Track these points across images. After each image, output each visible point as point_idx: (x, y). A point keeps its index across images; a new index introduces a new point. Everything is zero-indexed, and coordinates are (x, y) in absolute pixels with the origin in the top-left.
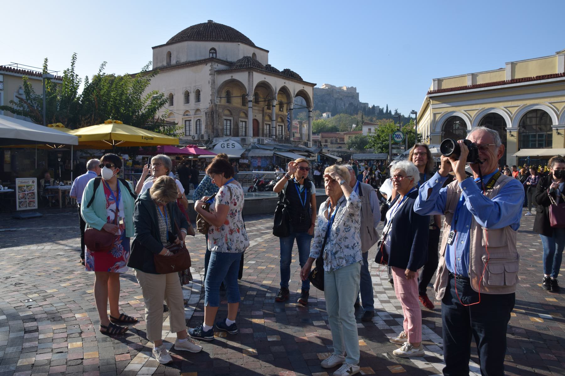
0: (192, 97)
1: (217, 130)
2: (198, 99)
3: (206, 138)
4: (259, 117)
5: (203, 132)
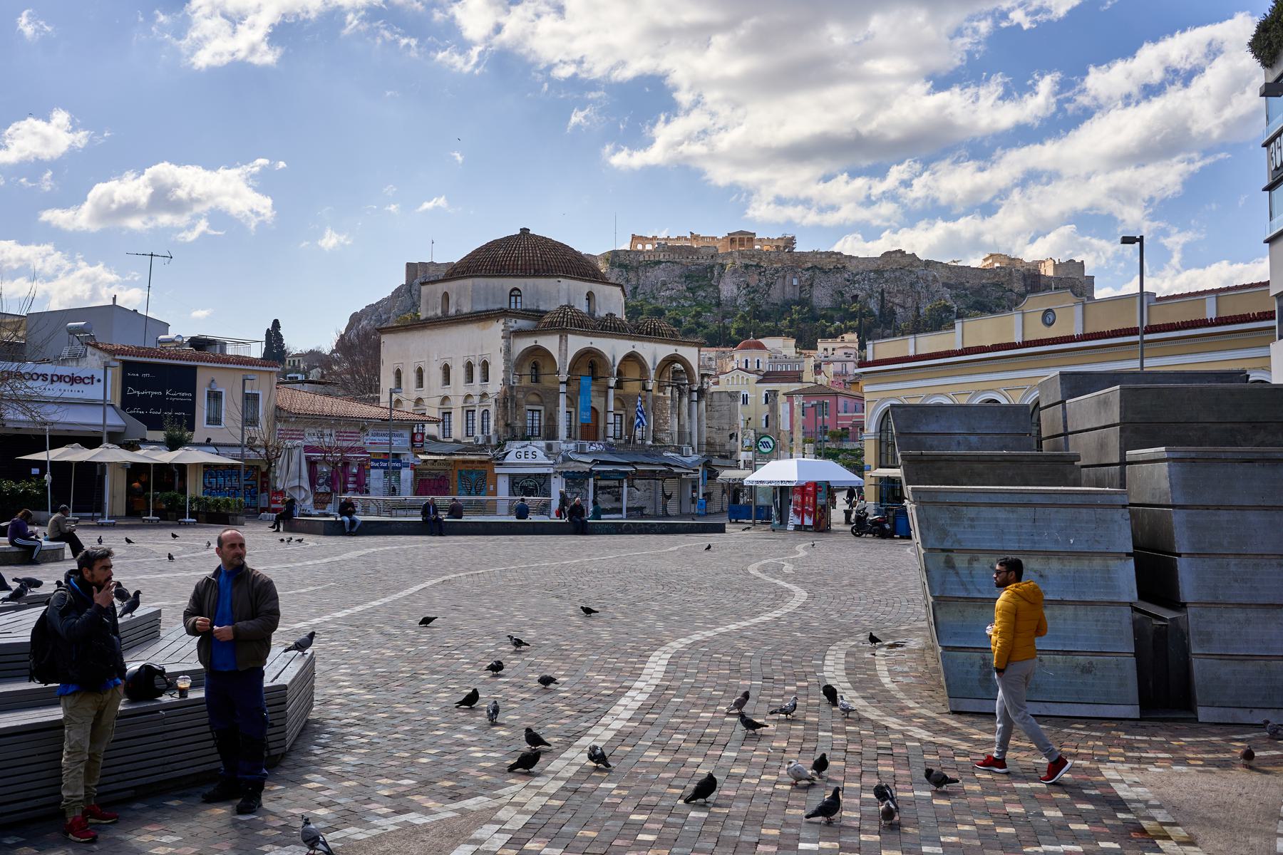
1: (513, 429)
3: (494, 442)
4: (598, 403)
5: (491, 433)
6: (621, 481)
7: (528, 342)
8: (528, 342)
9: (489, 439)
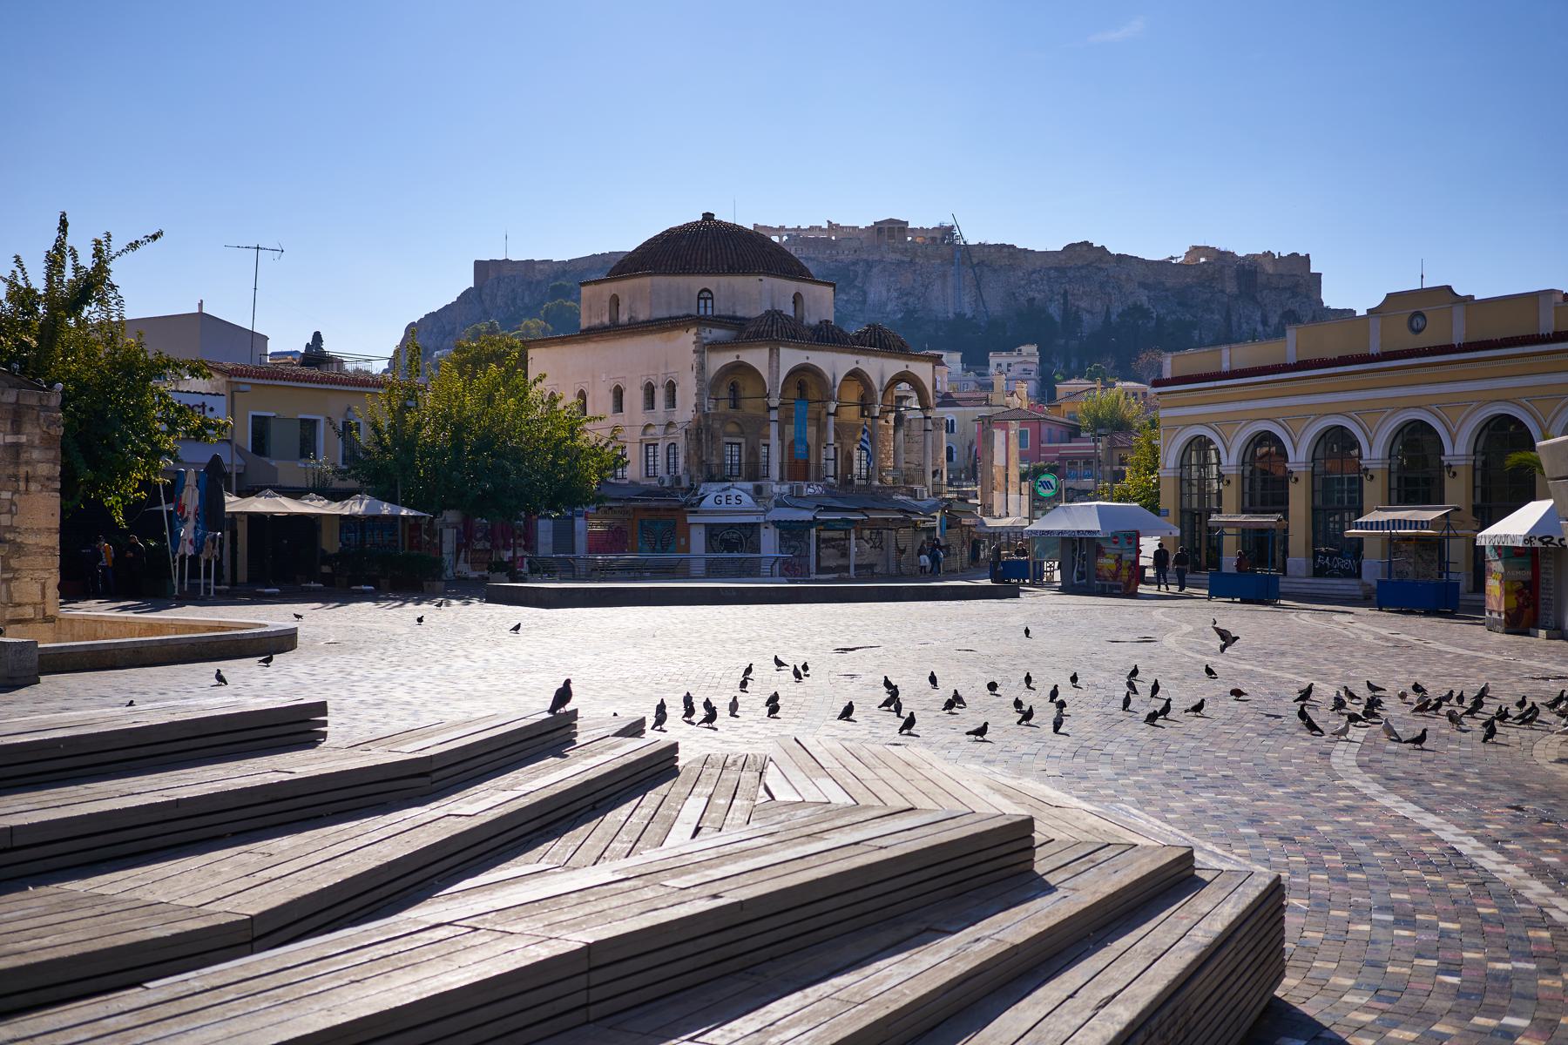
0: (660, 396)
1: (709, 467)
2: (671, 401)
3: (685, 484)
5: (680, 470)
6: (847, 532)
7: (728, 357)
8: (728, 357)
9: (678, 480)
